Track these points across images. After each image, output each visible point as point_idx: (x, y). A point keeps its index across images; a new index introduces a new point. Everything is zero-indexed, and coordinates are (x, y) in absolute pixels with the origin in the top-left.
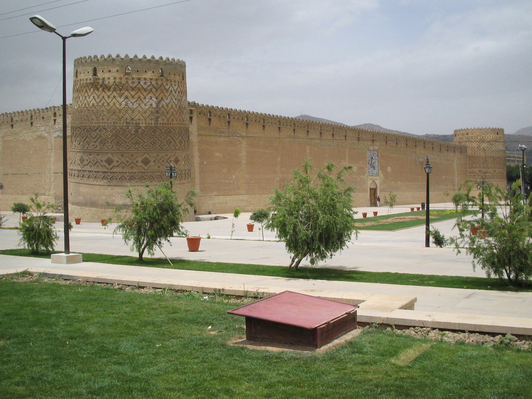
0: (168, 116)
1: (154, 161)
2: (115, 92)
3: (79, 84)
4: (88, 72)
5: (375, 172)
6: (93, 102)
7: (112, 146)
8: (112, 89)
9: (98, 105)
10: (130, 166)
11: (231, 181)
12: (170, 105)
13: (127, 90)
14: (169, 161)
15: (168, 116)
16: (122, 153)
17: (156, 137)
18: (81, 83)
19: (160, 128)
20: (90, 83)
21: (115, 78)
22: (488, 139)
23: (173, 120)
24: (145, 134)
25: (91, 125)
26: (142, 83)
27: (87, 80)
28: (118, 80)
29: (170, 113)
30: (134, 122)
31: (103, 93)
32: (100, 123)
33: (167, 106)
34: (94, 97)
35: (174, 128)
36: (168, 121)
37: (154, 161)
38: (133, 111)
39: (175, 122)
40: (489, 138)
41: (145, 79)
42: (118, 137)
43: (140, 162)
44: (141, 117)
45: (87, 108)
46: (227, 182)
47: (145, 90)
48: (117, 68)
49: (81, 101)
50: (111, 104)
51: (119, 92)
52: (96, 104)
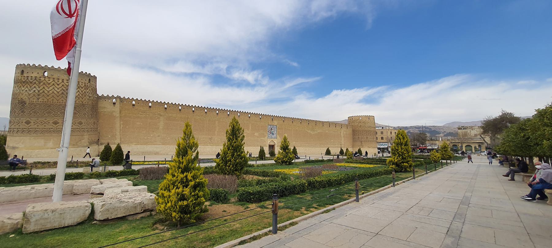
0: (48, 98)
1: (34, 123)
5: (273, 136)
10: (18, 125)
11: (149, 138)
15: (48, 98)
23: (53, 100)
26: (29, 78)
28: (18, 78)
33: (48, 92)
35: (54, 105)
36: (48, 100)
39: (55, 100)
40: (364, 120)
41: (32, 77)
47: (31, 83)
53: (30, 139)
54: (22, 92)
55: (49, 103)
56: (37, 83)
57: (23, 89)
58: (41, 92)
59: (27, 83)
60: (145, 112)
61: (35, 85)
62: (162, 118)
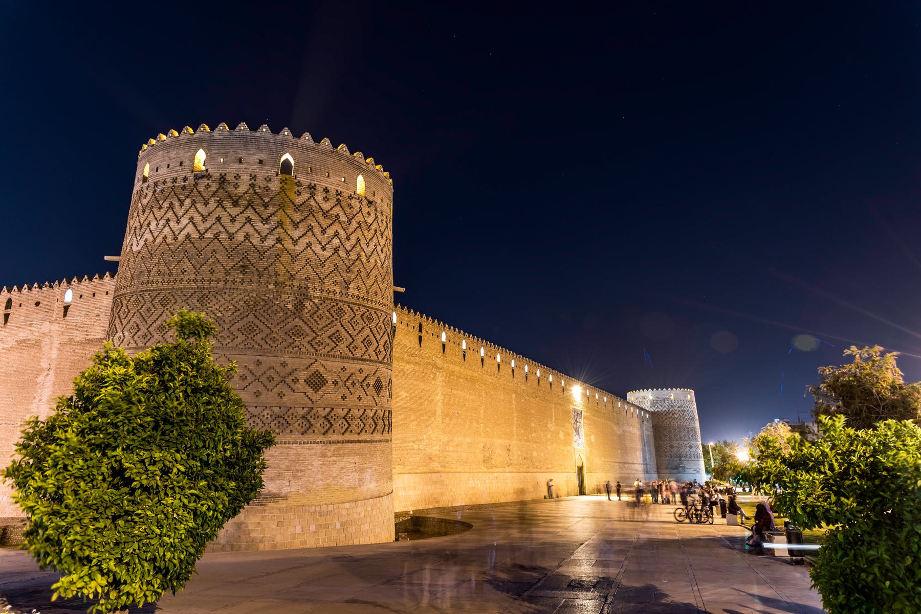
0: (369, 282)
1: (335, 383)
2: (250, 209)
3: (150, 194)
4: (181, 164)
6: (190, 229)
7: (232, 337)
8: (244, 202)
9: (201, 236)
12: (372, 260)
13: (282, 207)
14: (364, 384)
15: (369, 282)
16: (259, 358)
17: (342, 326)
18: (158, 190)
19: (351, 306)
20: (184, 188)
21: (253, 177)
22: (678, 405)
24: (318, 314)
25: (176, 286)
26: (319, 197)
27: (175, 180)
29: (372, 277)
30: (296, 283)
31: (220, 209)
32: (203, 280)
34: (191, 219)
36: (368, 292)
37: (335, 383)
38: (294, 259)
40: (680, 402)
41: (326, 190)
42: (251, 316)
43: (301, 381)
44: (312, 275)
45: (168, 245)
46: (416, 447)
47: (325, 214)
48: (262, 156)
49: (151, 231)
50: (240, 237)
51: (262, 209)
52: (195, 235)
53: (324, 456)
54: (288, 244)
55: (369, 304)
56: (343, 218)
57: (295, 237)
58: (353, 256)
59: (312, 212)
60: (412, 355)
61: (336, 227)
62: (440, 377)
